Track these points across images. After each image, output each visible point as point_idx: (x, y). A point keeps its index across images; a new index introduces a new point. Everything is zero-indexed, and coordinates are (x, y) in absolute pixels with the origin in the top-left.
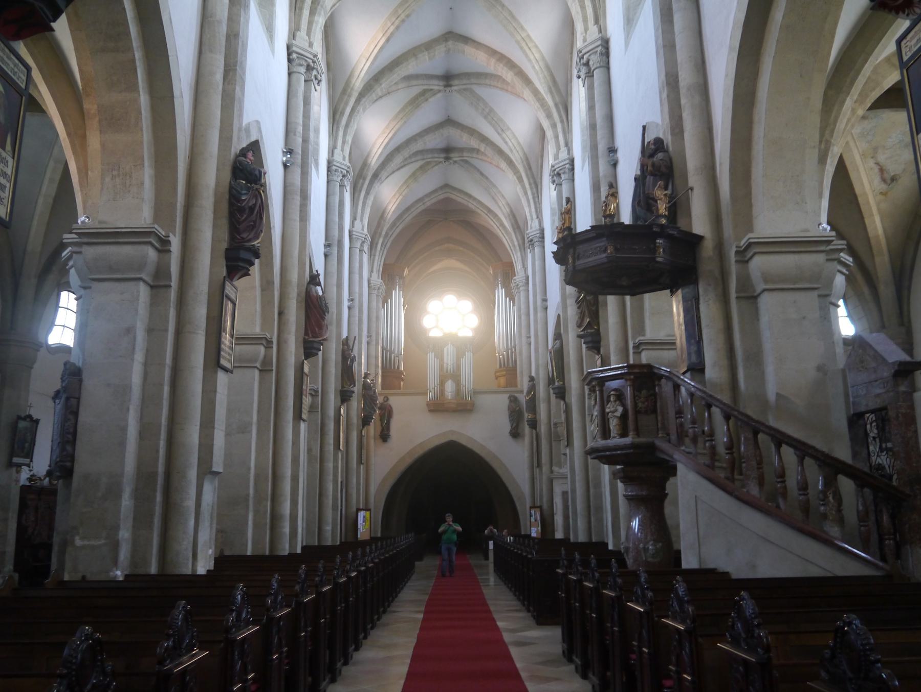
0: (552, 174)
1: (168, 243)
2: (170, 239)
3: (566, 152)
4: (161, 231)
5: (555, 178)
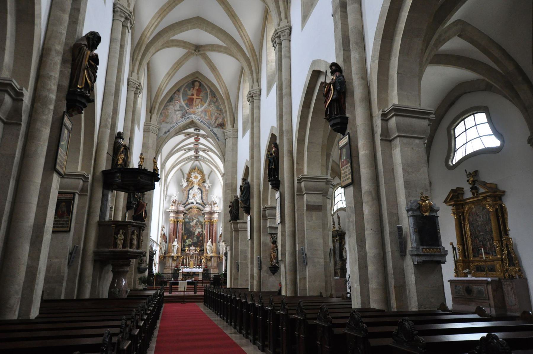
0: (249, 96)
1: (22, 95)
2: (23, 92)
3: (257, 86)
4: (16, 84)
5: (250, 98)
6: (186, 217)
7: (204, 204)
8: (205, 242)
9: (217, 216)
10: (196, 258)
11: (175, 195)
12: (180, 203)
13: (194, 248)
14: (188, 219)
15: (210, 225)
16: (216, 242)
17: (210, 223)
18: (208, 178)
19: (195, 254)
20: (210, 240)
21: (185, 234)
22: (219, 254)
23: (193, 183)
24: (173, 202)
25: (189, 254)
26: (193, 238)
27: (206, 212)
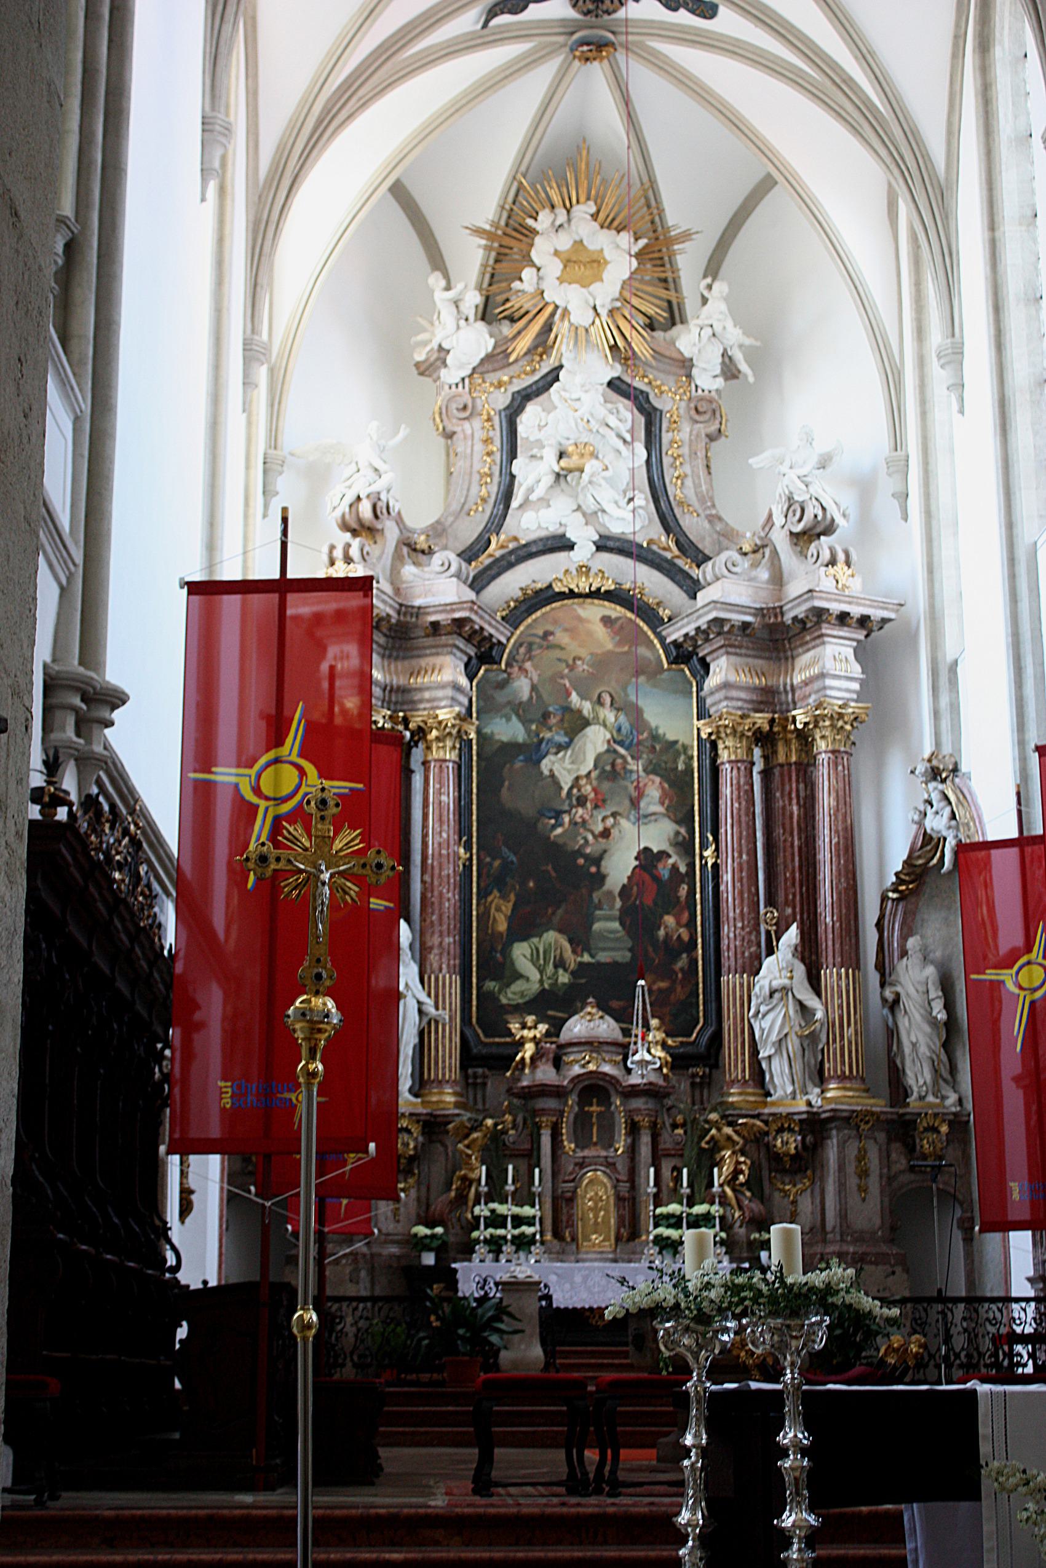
6: (501, 697)
7: (686, 547)
8: (728, 958)
9: (856, 670)
10: (645, 1139)
11: (366, 454)
12: (421, 541)
13: (606, 1028)
14: (521, 710)
15: (766, 774)
16: (852, 959)
17: (765, 757)
18: (713, 269)
19: (633, 1092)
20: (792, 935)
21: (493, 882)
22: (898, 1089)
23: (548, 327)
24: (345, 526)
25: (558, 1092)
26: (588, 921)
27: (718, 622)
